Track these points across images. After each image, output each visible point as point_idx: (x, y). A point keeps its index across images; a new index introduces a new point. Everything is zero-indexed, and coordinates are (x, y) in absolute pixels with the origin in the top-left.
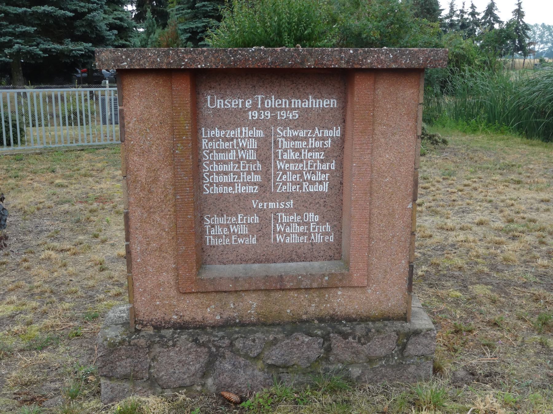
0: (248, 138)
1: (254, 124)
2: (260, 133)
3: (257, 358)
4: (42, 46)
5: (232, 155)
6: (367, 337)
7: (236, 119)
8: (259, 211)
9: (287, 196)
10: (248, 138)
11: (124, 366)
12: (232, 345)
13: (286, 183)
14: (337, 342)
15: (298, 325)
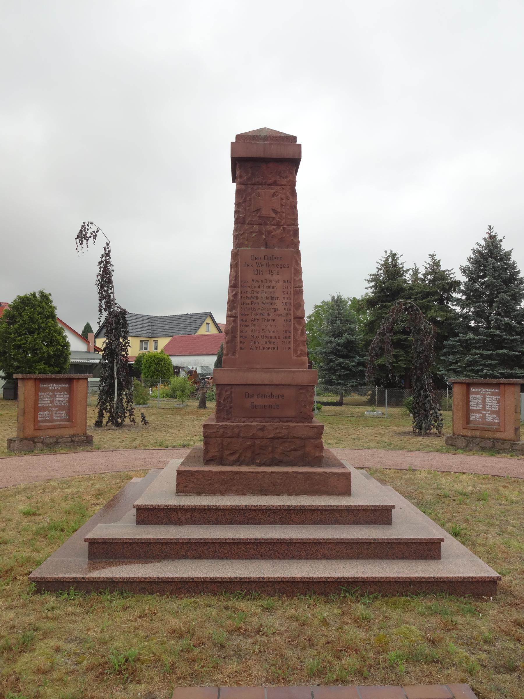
0: (480, 397)
1: (481, 394)
2: (482, 396)
3: (478, 444)
4: (500, 371)
5: (476, 401)
6: (503, 443)
7: (477, 393)
8: (482, 413)
9: (488, 411)
10: (480, 397)
11: (450, 442)
12: (472, 440)
13: (488, 407)
14: (496, 443)
15: (489, 439)
